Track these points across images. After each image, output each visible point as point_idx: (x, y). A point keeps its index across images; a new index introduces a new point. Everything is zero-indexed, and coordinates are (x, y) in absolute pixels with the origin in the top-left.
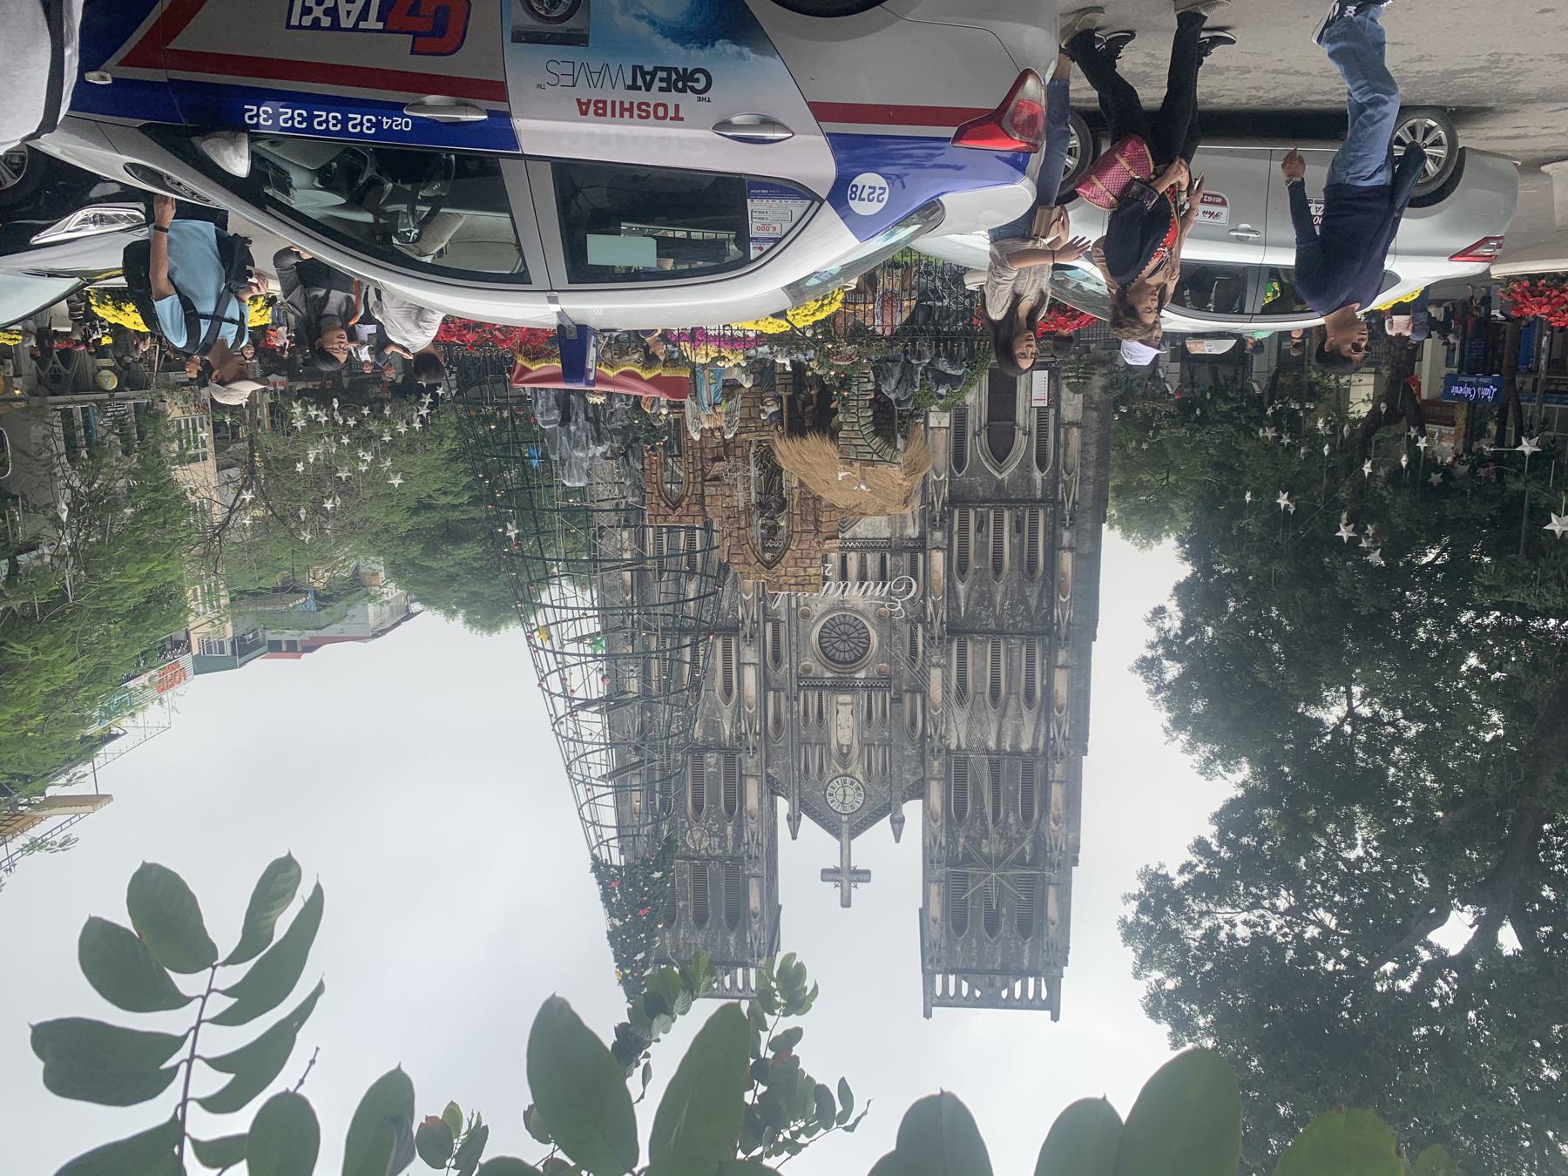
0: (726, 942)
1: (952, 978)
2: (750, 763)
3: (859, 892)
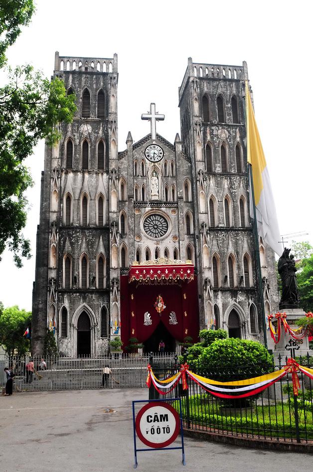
1: (105, 71)
2: (201, 167)
3: (145, 110)
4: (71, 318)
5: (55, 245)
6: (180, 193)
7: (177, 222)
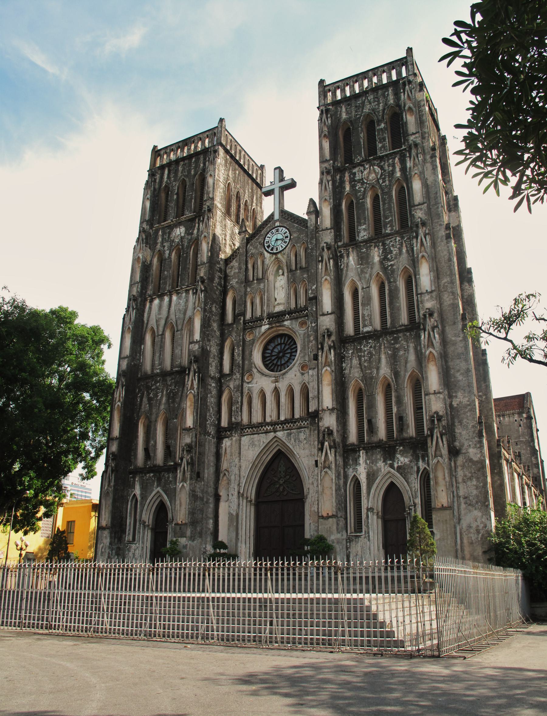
0: (347, 113)
4: (142, 511)
6: (313, 290)
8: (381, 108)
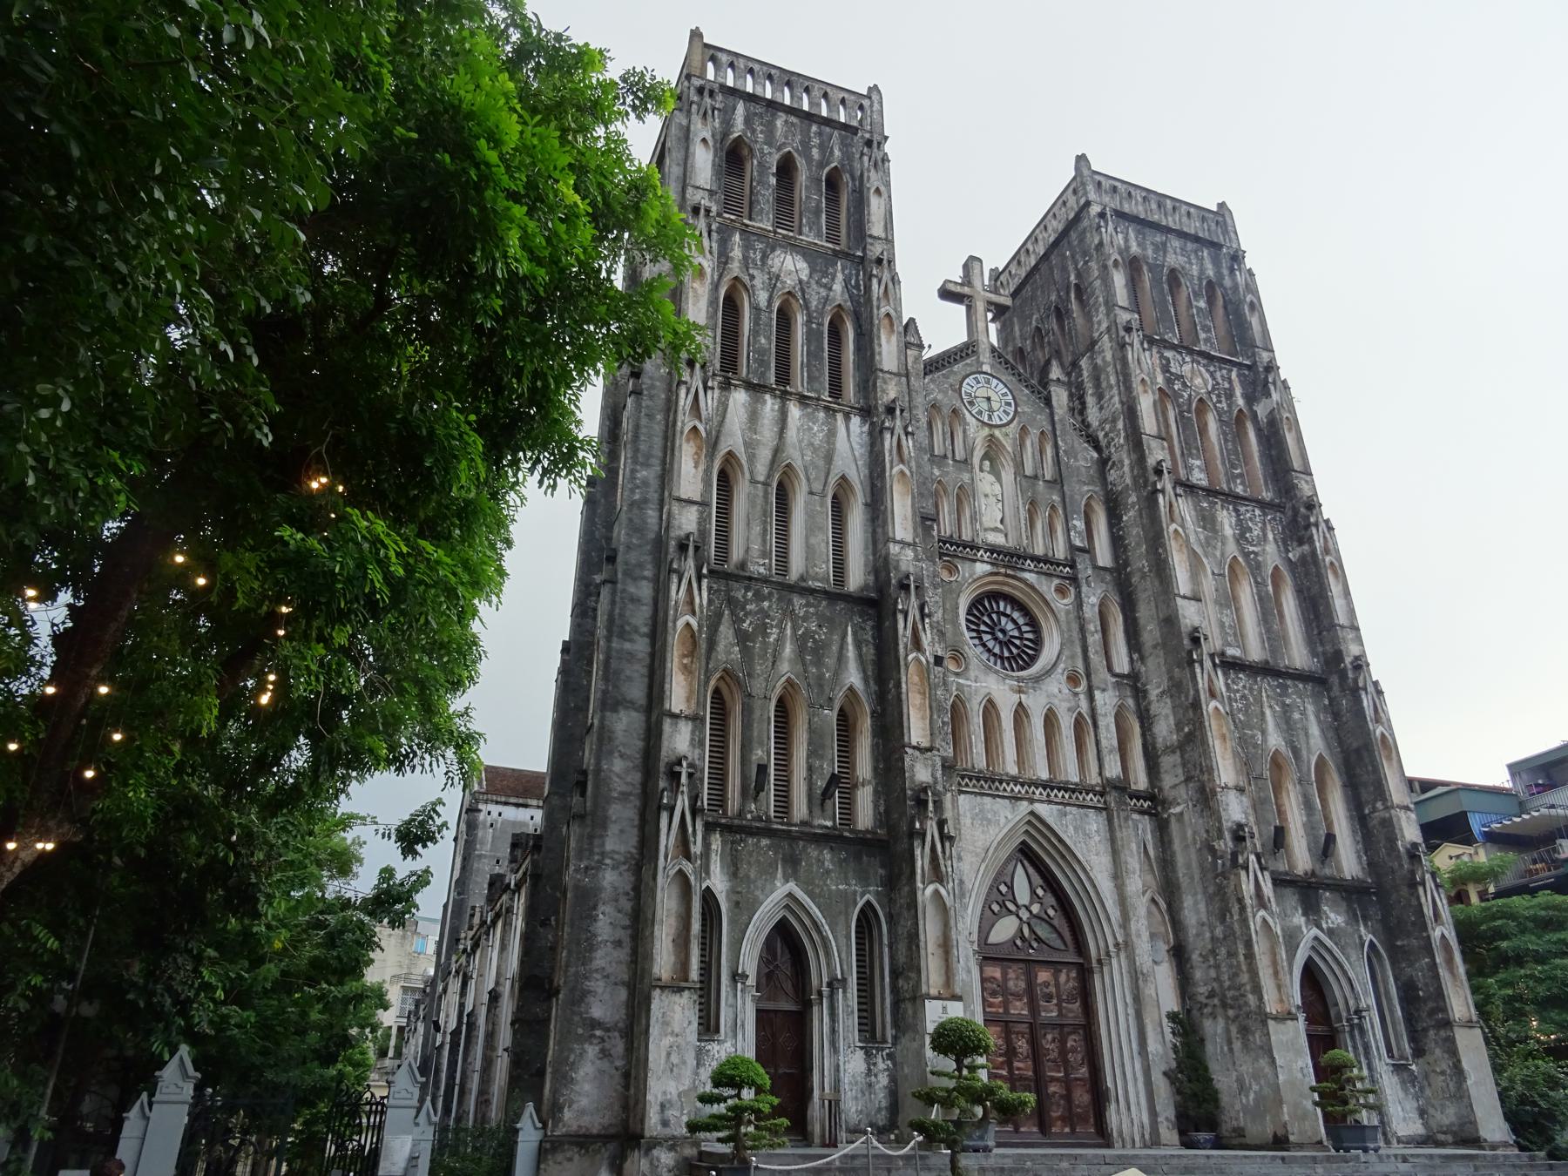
5: (694, 623)
7: (1075, 626)
8: (1195, 273)
